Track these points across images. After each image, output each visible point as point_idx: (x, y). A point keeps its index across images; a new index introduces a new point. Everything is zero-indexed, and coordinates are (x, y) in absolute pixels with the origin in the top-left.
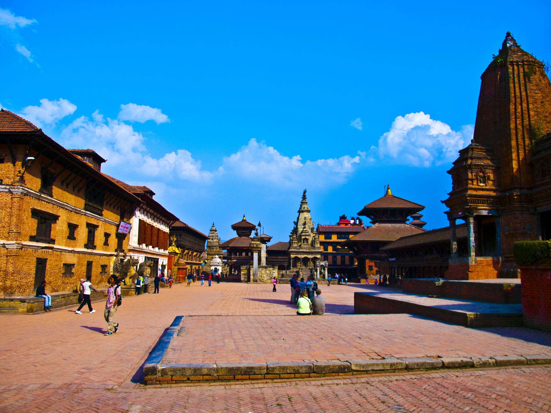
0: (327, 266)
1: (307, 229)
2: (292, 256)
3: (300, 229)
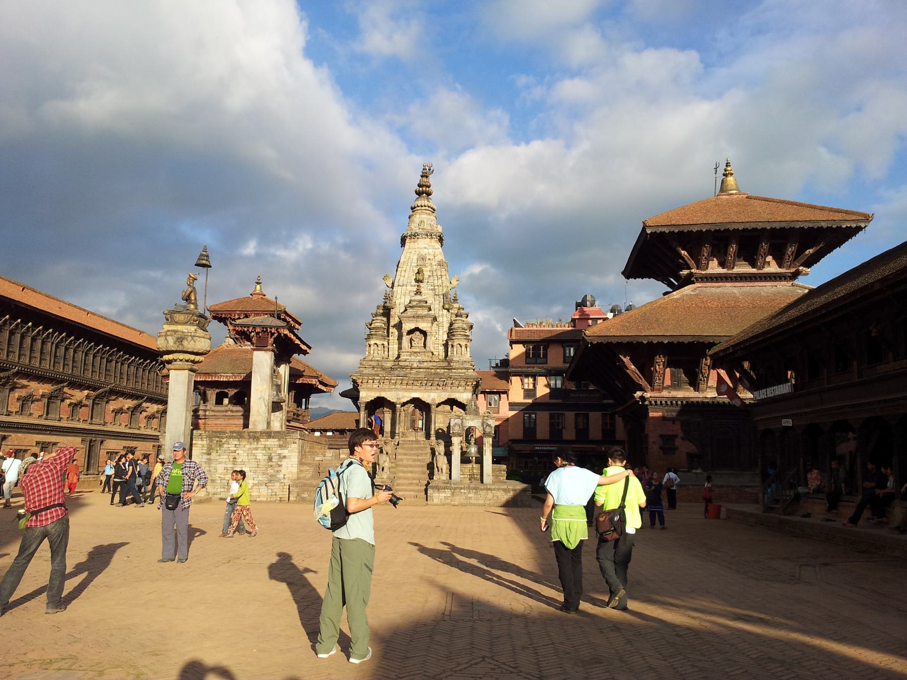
1: (427, 294)
3: (401, 300)
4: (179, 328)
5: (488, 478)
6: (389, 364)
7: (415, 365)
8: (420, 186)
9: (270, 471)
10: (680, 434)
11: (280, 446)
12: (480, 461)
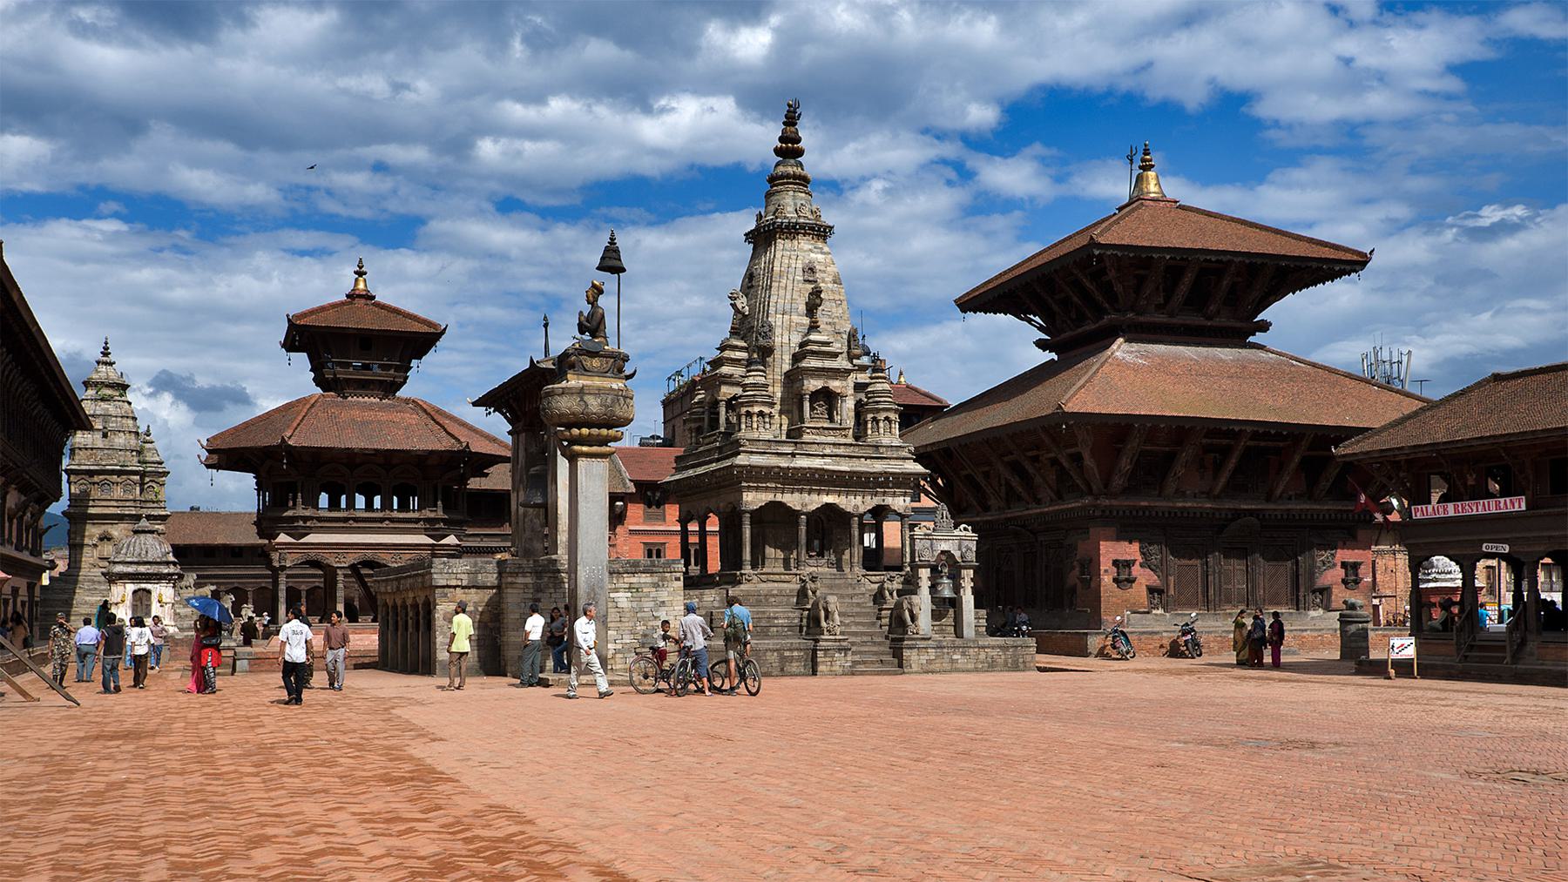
0: (971, 556)
2: (753, 499)
4: (597, 382)
5: (969, 631)
6: (788, 449)
7: (828, 451)
8: (781, 139)
9: (640, 628)
10: (1140, 559)
11: (656, 585)
12: (955, 603)
